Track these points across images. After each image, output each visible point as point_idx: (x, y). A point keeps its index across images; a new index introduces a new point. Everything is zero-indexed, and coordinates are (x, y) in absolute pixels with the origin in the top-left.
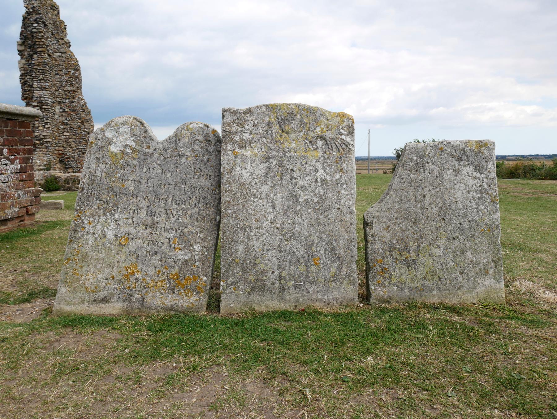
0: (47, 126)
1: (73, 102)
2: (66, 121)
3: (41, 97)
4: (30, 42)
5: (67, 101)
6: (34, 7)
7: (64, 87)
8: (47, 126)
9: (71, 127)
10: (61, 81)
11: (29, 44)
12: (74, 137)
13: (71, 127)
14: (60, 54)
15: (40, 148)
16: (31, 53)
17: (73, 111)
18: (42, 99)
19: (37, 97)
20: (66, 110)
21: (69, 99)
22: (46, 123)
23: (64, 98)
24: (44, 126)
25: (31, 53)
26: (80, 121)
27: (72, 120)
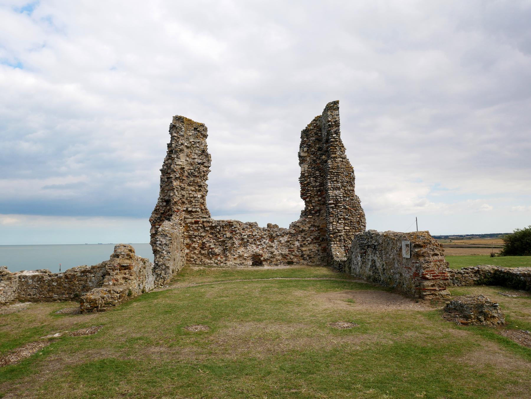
0: (340, 222)
1: (352, 200)
2: (347, 217)
3: (337, 196)
4: (313, 149)
5: (347, 199)
6: (336, 121)
7: (345, 187)
8: (340, 222)
9: (351, 222)
10: (342, 182)
11: (313, 151)
12: (354, 231)
13: (351, 222)
14: (341, 159)
15: (334, 241)
16: (314, 158)
17: (353, 207)
18: (338, 197)
19: (333, 196)
20: (347, 207)
21: (349, 197)
22: (340, 219)
23: (344, 197)
24: (338, 221)
25: (314, 158)
26: (359, 216)
27: (353, 215)
